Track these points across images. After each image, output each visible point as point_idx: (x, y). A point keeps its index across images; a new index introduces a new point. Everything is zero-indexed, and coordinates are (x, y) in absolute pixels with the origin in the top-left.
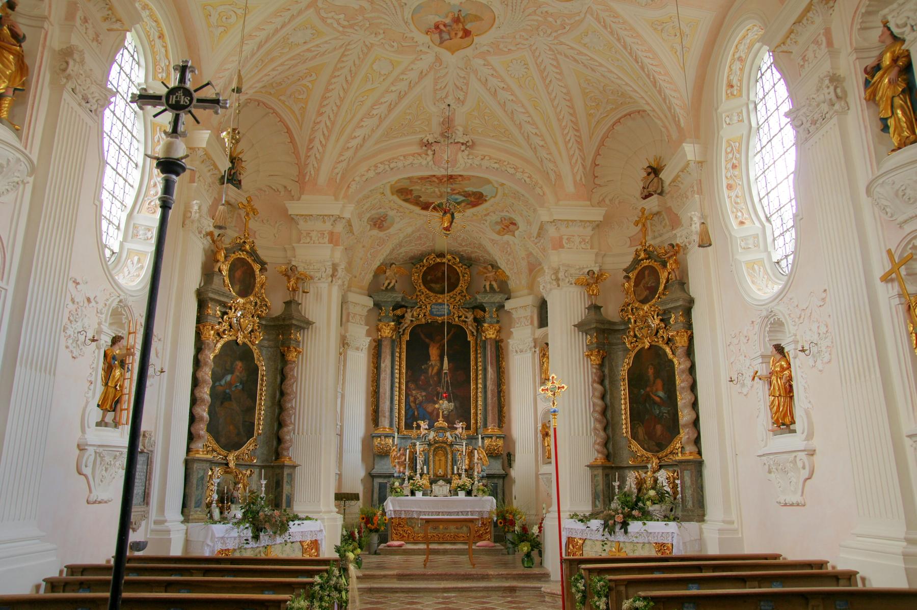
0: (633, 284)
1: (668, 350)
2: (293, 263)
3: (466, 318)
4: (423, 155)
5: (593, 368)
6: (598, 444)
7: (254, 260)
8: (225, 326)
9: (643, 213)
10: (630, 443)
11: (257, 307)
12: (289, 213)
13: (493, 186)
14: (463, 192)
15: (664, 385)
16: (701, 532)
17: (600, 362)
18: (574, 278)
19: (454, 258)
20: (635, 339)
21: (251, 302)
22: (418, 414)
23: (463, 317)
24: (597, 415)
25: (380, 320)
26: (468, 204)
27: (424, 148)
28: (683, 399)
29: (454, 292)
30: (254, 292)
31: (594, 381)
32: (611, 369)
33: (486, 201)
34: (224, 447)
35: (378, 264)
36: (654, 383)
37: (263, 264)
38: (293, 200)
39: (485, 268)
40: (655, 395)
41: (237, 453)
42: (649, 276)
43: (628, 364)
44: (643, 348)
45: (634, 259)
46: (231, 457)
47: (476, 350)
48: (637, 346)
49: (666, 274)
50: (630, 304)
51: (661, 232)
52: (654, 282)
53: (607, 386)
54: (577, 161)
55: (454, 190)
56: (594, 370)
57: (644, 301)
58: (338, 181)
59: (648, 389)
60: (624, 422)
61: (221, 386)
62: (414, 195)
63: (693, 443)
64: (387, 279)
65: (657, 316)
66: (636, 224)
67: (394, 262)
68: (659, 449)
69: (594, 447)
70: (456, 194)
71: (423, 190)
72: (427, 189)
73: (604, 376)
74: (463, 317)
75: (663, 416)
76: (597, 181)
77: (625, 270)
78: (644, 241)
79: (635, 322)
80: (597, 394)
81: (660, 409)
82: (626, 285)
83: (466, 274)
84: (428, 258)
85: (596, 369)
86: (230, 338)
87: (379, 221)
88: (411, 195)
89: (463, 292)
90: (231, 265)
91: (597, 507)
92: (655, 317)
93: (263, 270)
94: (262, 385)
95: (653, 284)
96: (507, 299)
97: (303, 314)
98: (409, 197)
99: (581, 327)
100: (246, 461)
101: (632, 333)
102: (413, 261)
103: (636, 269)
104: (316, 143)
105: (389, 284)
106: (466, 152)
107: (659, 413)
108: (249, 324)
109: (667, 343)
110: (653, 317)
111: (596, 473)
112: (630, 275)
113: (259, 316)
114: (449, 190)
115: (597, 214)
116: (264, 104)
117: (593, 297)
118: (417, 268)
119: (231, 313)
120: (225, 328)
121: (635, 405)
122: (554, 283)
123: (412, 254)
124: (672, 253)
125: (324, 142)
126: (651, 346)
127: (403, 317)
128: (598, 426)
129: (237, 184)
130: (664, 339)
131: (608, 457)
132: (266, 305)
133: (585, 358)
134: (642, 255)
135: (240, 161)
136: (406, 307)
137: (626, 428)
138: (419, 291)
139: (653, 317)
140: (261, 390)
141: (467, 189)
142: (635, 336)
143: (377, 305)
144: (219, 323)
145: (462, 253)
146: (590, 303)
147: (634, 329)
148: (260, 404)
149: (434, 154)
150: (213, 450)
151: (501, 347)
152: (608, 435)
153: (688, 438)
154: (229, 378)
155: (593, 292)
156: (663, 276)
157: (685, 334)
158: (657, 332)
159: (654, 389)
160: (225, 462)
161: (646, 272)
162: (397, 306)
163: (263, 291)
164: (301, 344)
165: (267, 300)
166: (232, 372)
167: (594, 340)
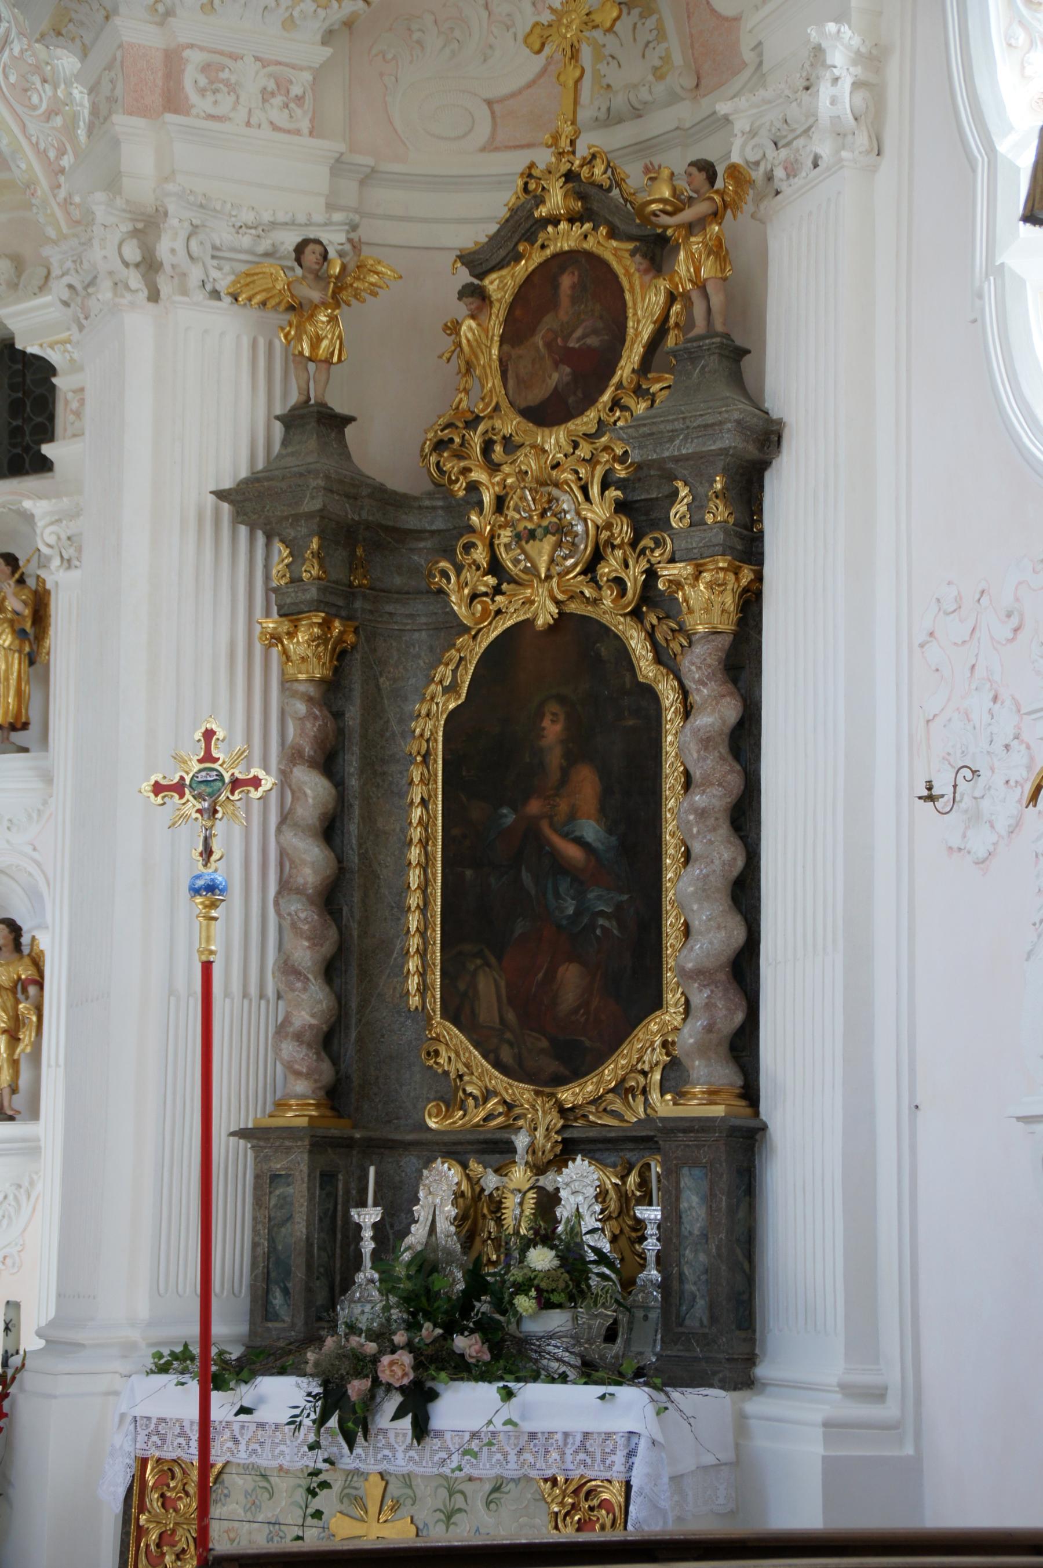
0: (497, 329)
5: (294, 694)
6: (298, 1037)
15: (606, 793)
17: (328, 673)
18: (227, 268)
20: (491, 580)
32: (373, 709)
40: (565, 836)
42: (574, 300)
44: (529, 623)
45: (514, 211)
48: (499, 612)
49: (656, 300)
50: (478, 419)
51: (644, 94)
52: (595, 332)
53: (354, 783)
56: (301, 708)
59: (534, 807)
60: (414, 943)
65: (605, 486)
68: (563, 1070)
69: (277, 1050)
73: (341, 732)
75: (592, 926)
78: (568, 129)
79: (500, 503)
82: (468, 328)
85: (310, 700)
91: (276, 1317)
92: (595, 491)
95: (593, 341)
101: (480, 555)
103: (517, 258)
107: (578, 913)
109: (636, 614)
110: (585, 490)
111: (278, 1165)
112: (492, 283)
117: (311, 366)
121: (469, 873)
126: (563, 617)
130: (623, 592)
134: (556, 200)
139: (585, 490)
142: (495, 567)
146: (294, 398)
147: (493, 536)
152: (341, 1000)
158: (597, 557)
159: (563, 807)
161: (566, 281)
167: (310, 571)
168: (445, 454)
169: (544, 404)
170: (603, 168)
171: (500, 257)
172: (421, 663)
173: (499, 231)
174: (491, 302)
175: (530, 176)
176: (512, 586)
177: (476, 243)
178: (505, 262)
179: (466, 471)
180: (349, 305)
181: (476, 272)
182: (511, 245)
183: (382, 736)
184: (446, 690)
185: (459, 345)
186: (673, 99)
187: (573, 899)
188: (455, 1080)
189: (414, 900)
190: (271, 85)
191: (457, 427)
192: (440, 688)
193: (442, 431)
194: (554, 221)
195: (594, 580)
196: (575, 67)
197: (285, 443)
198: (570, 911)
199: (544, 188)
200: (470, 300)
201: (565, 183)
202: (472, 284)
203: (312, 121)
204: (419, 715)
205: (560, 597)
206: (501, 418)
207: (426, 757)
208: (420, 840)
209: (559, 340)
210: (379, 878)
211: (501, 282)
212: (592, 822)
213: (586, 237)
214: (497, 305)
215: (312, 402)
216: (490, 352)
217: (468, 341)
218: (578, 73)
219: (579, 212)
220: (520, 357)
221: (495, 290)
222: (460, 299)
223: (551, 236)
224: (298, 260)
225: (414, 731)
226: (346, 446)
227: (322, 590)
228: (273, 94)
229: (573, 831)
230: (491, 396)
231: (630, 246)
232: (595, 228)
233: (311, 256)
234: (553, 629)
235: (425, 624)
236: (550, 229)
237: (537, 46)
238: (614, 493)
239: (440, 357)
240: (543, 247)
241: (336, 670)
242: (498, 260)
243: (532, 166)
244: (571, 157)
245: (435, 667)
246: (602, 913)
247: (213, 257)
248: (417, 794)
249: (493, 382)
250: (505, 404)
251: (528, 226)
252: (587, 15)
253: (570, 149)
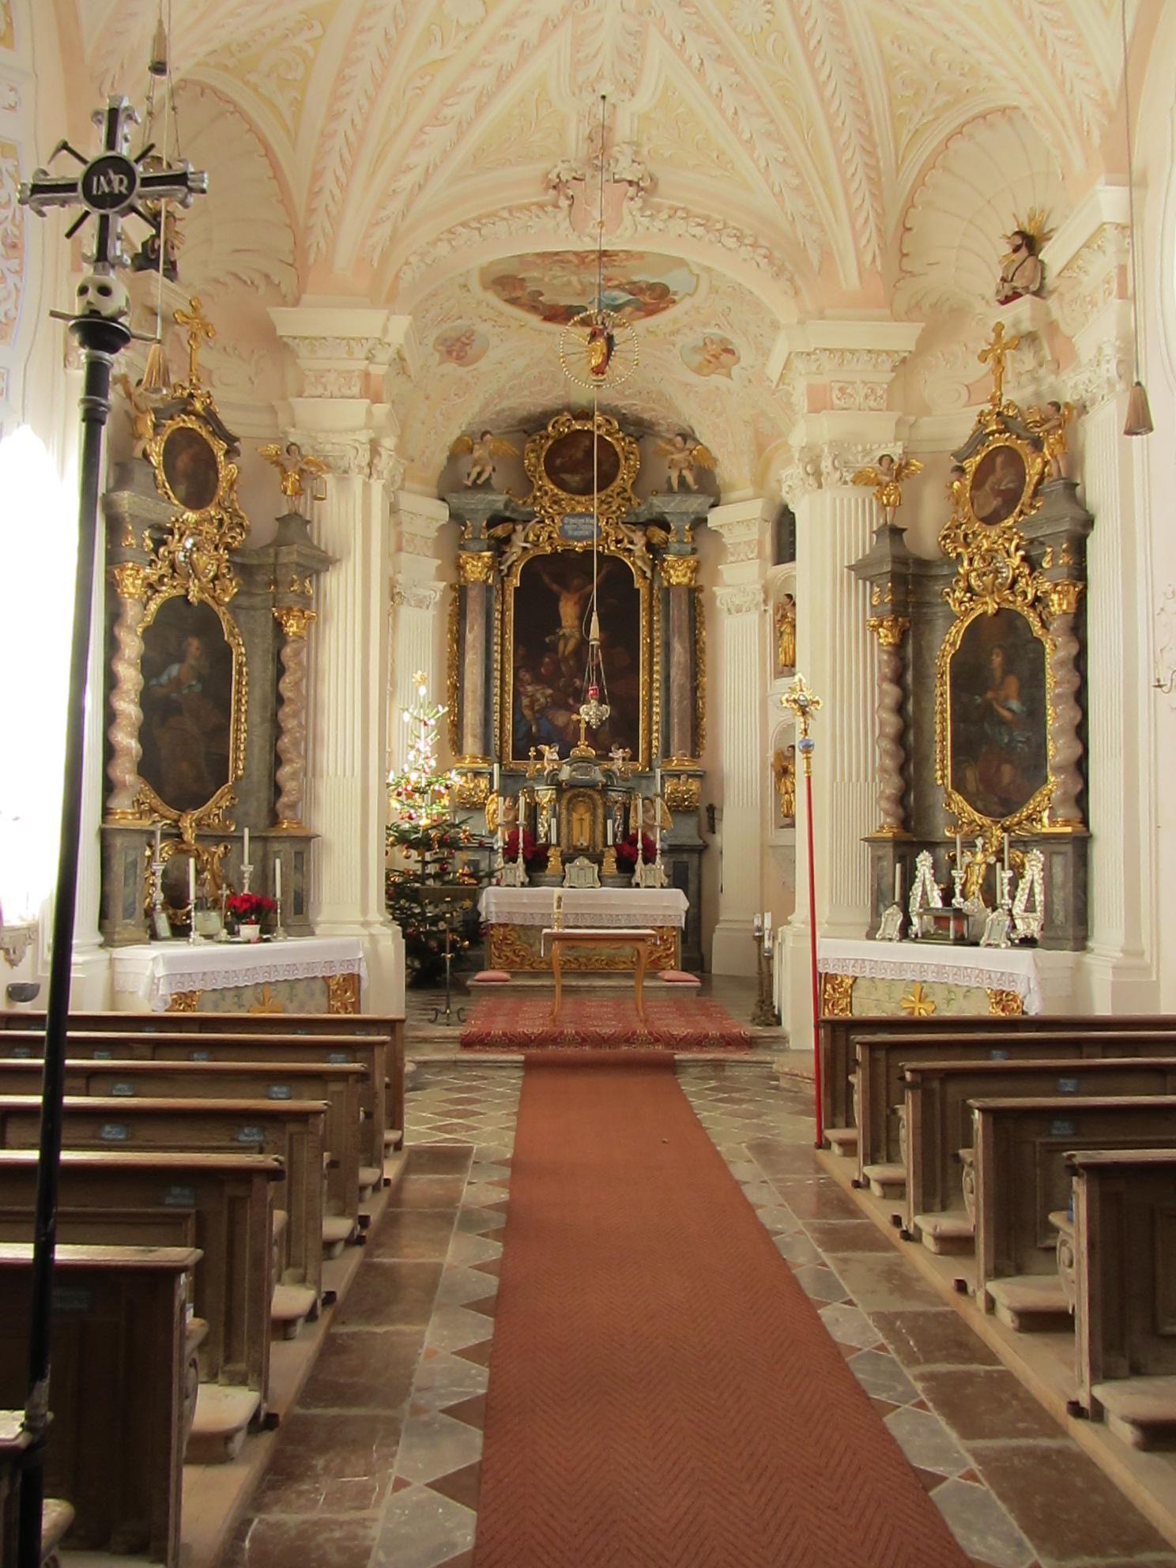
0: (968, 483)
2: (292, 440)
3: (631, 542)
4: (550, 209)
6: (888, 799)
7: (213, 433)
8: (163, 567)
9: (999, 336)
11: (225, 529)
12: (280, 332)
13: (691, 272)
14: (628, 284)
15: (1021, 688)
16: (1078, 969)
17: (897, 640)
19: (607, 421)
20: (968, 595)
21: (212, 518)
22: (539, 730)
23: (626, 541)
24: (887, 744)
25: (462, 547)
26: (638, 309)
27: (552, 192)
28: (1056, 717)
29: (609, 491)
30: (216, 500)
31: (883, 678)
33: (674, 302)
34: (172, 803)
35: (457, 433)
36: (1002, 683)
37: (230, 439)
38: (285, 304)
39: (670, 442)
40: (1003, 707)
41: (197, 813)
42: (1002, 468)
43: (953, 644)
44: (985, 613)
46: (187, 823)
47: (651, 607)
52: (1012, 481)
54: (867, 220)
55: (610, 280)
56: (885, 657)
57: (991, 520)
58: (376, 265)
59: (989, 695)
61: (161, 686)
62: (528, 290)
63: (1072, 802)
64: (475, 465)
66: (983, 357)
67: (489, 429)
68: (1004, 811)
70: (617, 287)
71: (547, 279)
72: (555, 277)
74: (626, 541)
75: (1016, 748)
76: (907, 265)
77: (955, 455)
80: (889, 701)
81: (1011, 735)
82: (956, 484)
83: (632, 453)
84: (556, 422)
85: (889, 653)
86: (175, 592)
87: (459, 344)
88: (523, 288)
89: (625, 490)
90: (166, 443)
93: (231, 453)
94: (239, 683)
95: (1011, 485)
96: (714, 506)
97: (316, 543)
98: (518, 293)
99: (861, 570)
100: (214, 829)
102: (526, 427)
103: (978, 453)
104: (329, 181)
105: (479, 475)
106: (639, 203)
107: (1009, 742)
108: (208, 563)
109: (1032, 606)
111: (880, 853)
112: (966, 464)
113: (227, 547)
114: (596, 279)
115: (903, 337)
116: (214, 91)
118: (534, 441)
119: (173, 541)
120: (162, 572)
121: (962, 725)
122: (811, 480)
123: (525, 413)
124: (1054, 423)
125: (343, 179)
126: (999, 611)
127: (507, 540)
128: (888, 763)
129: (171, 271)
131: (904, 823)
132: (241, 525)
135: (171, 219)
136: (514, 521)
138: (539, 489)
140: (239, 692)
141: (635, 278)
142: (969, 589)
143: (456, 517)
144: (152, 563)
145: (624, 411)
146: (882, 521)
148: (238, 720)
149: (571, 206)
150: (153, 810)
151: (699, 601)
153: (1064, 793)
154: (174, 670)
155: (888, 500)
156: (1033, 468)
157: (1072, 588)
158: (1015, 581)
160: (174, 831)
161: (999, 460)
162: (494, 521)
163: (234, 496)
164: (314, 601)
165: (242, 514)
166: (180, 658)
179: (955, 548)
184: (951, 645)
194: (992, 433)
227: (893, 605)
233: (885, 462)
238: (1021, 553)
248: (938, 691)
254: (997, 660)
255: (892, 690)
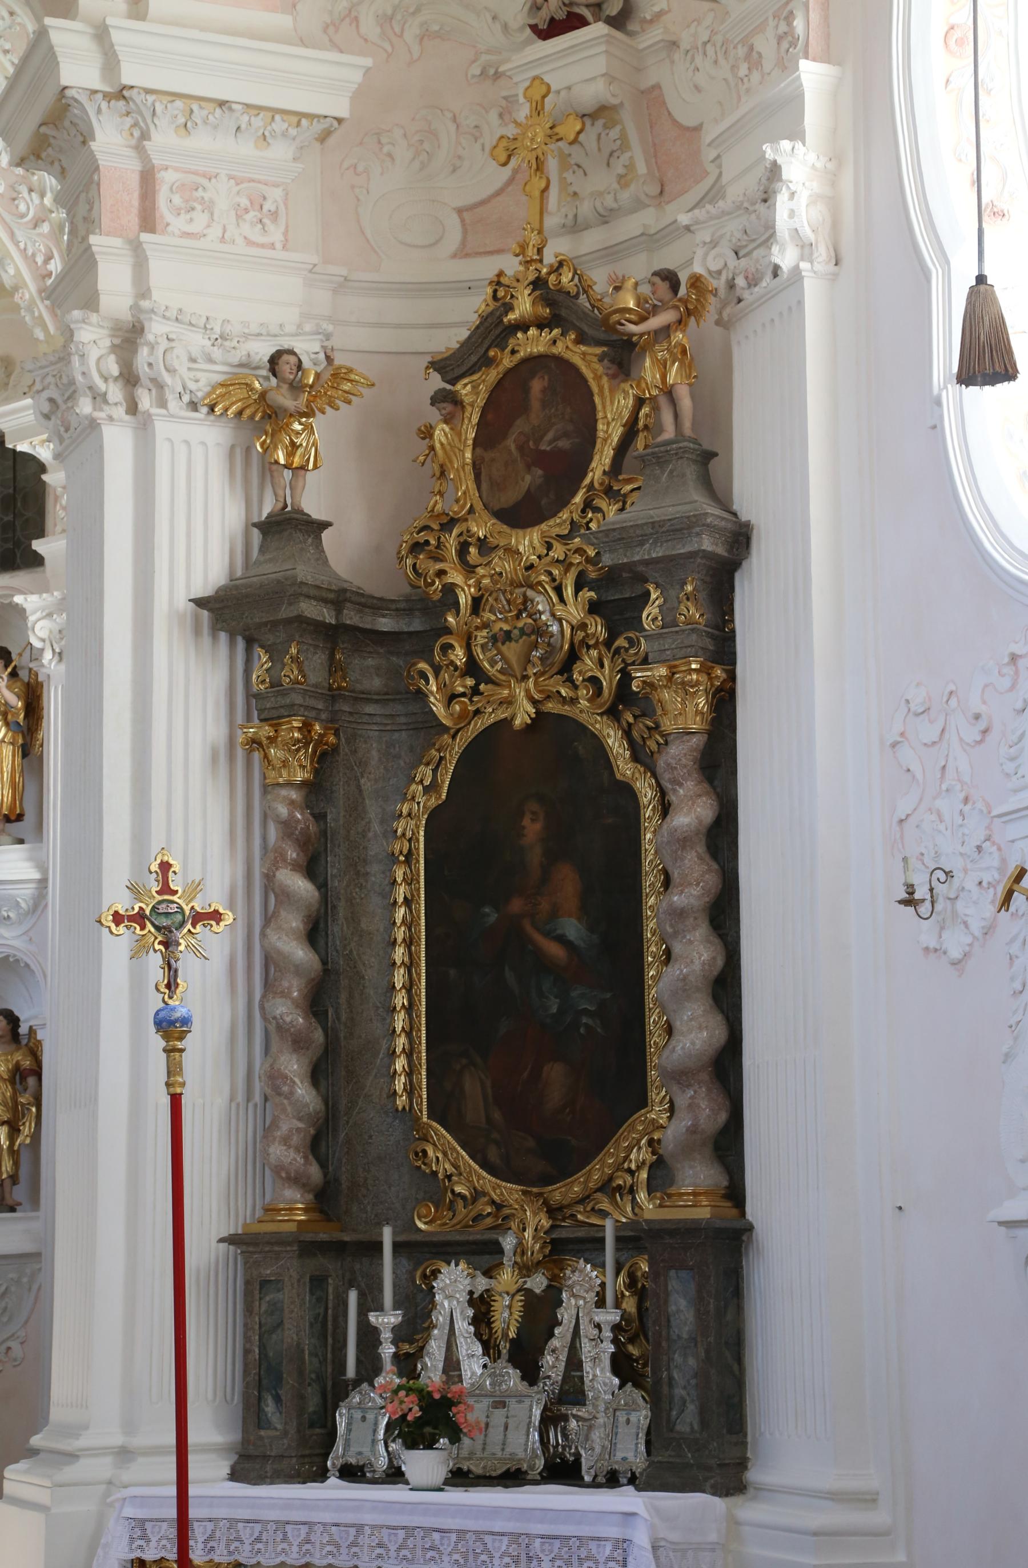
1: (614, 741)
6: (285, 1141)
9: (538, 109)
10: (425, 1139)
20: (470, 682)
31: (274, 859)
32: (356, 809)
40: (548, 934)
42: (544, 404)
44: (507, 723)
45: (484, 319)
48: (477, 712)
51: (609, 201)
52: (566, 435)
56: (283, 811)
59: (516, 905)
65: (578, 588)
78: (534, 239)
79: (477, 604)
82: (441, 433)
91: (269, 1425)
92: (569, 591)
95: (564, 444)
101: (459, 655)
103: (487, 362)
109: (612, 713)
110: (559, 590)
112: (464, 389)
121: (452, 972)
126: (540, 718)
133: (240, 753)
134: (524, 305)
137: (411, 1072)
139: (559, 590)
142: (472, 668)
155: (291, 453)
158: (573, 657)
161: (537, 385)
168: (421, 557)
169: (517, 506)
170: (570, 275)
171: (472, 363)
172: (402, 764)
173: (469, 338)
174: (463, 407)
175: (499, 283)
176: (490, 686)
177: (448, 349)
178: (477, 368)
179: (441, 573)
180: (324, 413)
181: (449, 378)
182: (482, 351)
183: (364, 837)
184: (427, 790)
185: (432, 448)
186: (639, 205)
187: (556, 997)
188: (443, 1180)
189: (400, 999)
190: (244, 202)
191: (432, 530)
192: (420, 788)
193: (418, 533)
194: (523, 326)
195: (570, 680)
196: (541, 178)
197: (262, 549)
198: (554, 1009)
199: (512, 296)
200: (445, 405)
201: (533, 291)
202: (444, 389)
203: (286, 234)
204: (400, 815)
205: (537, 696)
206: (476, 521)
207: (409, 856)
208: (404, 939)
209: (531, 443)
210: (363, 978)
211: (473, 387)
212: (574, 921)
213: (555, 342)
214: (469, 409)
215: (289, 509)
216: (464, 455)
217: (442, 444)
218: (543, 185)
219: (546, 318)
220: (493, 460)
221: (466, 395)
222: (432, 404)
223: (520, 342)
224: (274, 372)
225: (396, 831)
226: (323, 551)
228: (246, 211)
229: (556, 930)
230: (465, 499)
231: (598, 350)
232: (563, 334)
233: (286, 366)
234: (529, 729)
235: (405, 724)
236: (519, 335)
237: (503, 158)
238: (588, 594)
239: (414, 461)
240: (513, 352)
241: (316, 772)
242: (469, 365)
243: (500, 274)
244: (538, 266)
245: (415, 766)
246: (586, 1012)
247: (189, 369)
249: (468, 483)
250: (479, 506)
251: (497, 332)
252: (551, 128)
253: (535, 257)
254: (532, 828)
255: (301, 886)
